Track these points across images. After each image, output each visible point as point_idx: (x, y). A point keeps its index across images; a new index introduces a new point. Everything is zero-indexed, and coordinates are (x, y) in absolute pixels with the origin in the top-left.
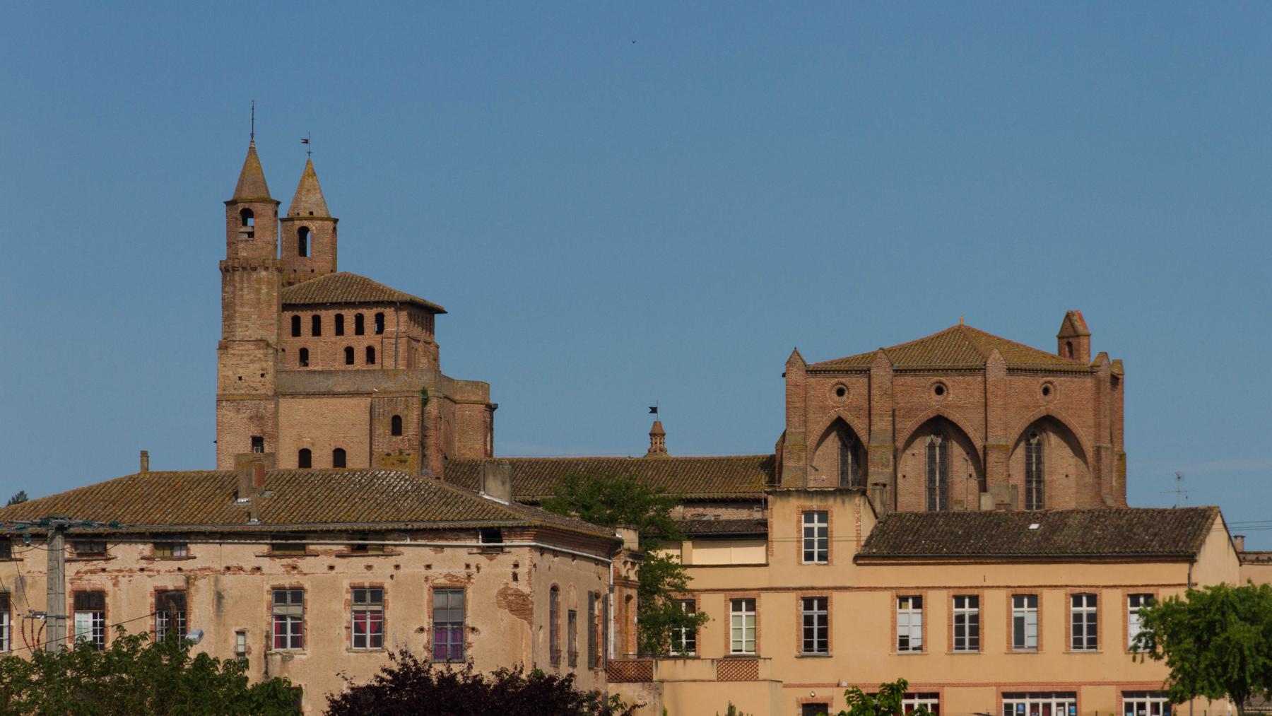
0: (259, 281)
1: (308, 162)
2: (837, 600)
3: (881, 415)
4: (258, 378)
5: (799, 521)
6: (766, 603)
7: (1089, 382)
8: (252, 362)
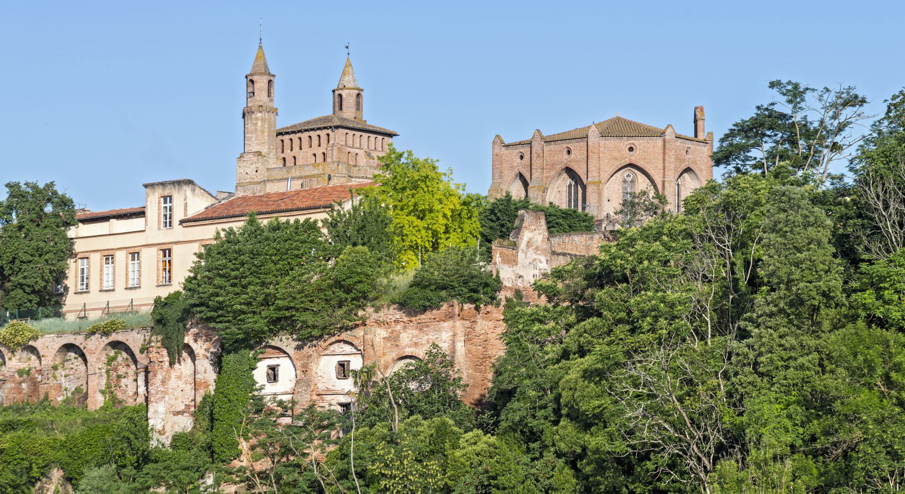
0: (257, 119)
1: (348, 59)
2: (176, 249)
3: (536, 169)
4: (254, 173)
5: (159, 203)
6: (144, 252)
7: (659, 142)
8: (252, 164)
